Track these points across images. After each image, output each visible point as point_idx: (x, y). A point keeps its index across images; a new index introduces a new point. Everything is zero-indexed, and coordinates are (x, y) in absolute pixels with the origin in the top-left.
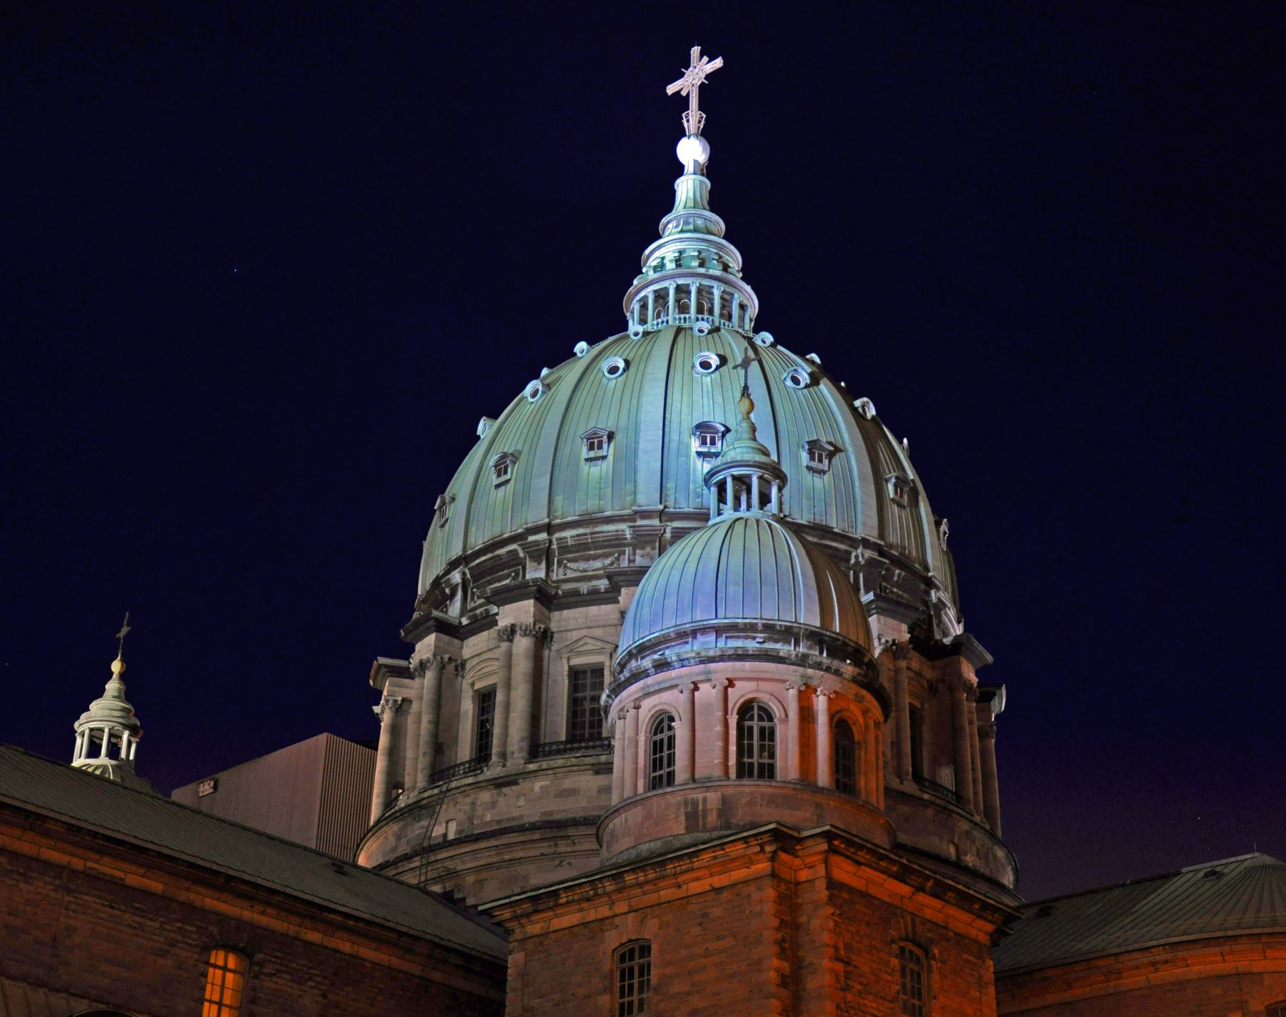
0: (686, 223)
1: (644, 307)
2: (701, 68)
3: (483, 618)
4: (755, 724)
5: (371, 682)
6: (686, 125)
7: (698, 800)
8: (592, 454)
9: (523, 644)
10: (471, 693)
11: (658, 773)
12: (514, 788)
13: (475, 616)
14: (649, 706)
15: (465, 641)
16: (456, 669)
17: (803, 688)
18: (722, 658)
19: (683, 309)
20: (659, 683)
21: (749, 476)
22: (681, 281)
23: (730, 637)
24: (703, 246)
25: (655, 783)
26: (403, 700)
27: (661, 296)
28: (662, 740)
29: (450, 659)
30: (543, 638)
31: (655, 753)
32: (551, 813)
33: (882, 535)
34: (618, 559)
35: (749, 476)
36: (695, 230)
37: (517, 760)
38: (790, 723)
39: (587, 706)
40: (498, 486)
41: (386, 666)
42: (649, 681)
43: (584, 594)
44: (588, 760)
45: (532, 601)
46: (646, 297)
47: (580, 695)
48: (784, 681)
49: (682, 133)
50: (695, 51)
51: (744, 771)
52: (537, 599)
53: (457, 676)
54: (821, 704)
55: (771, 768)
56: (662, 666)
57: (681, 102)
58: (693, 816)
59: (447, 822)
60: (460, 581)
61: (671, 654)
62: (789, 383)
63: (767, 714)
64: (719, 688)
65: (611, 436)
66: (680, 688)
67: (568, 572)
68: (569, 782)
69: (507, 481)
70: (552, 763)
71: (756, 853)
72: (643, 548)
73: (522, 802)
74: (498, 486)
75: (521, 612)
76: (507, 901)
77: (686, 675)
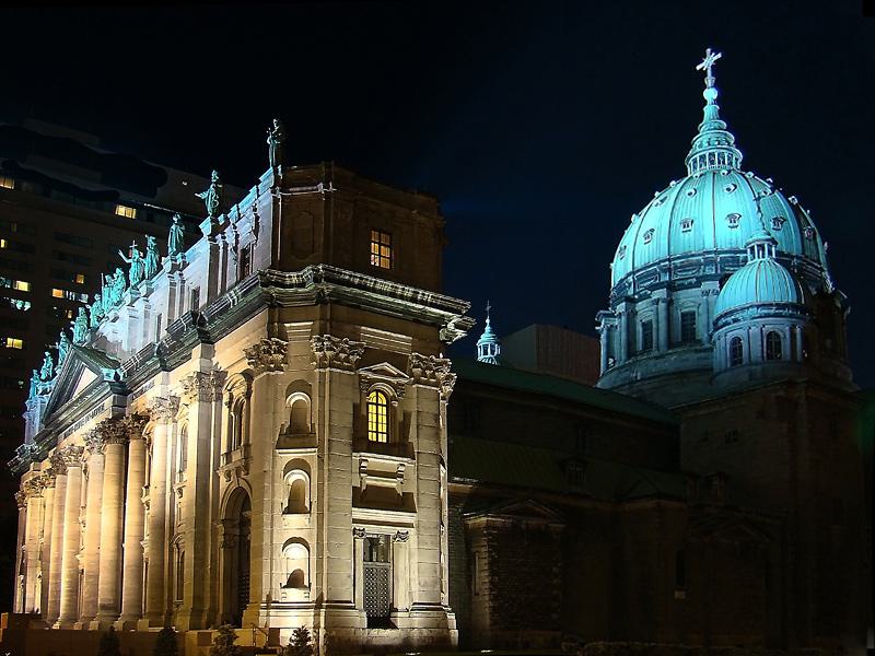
1: (695, 161)
2: (710, 60)
9: (662, 306)
14: (730, 336)
19: (712, 162)
27: (702, 157)
33: (803, 254)
37: (663, 349)
39: (689, 327)
49: (705, 87)
50: (709, 50)
54: (798, 330)
56: (735, 321)
57: (703, 73)
58: (752, 375)
63: (778, 336)
75: (661, 293)
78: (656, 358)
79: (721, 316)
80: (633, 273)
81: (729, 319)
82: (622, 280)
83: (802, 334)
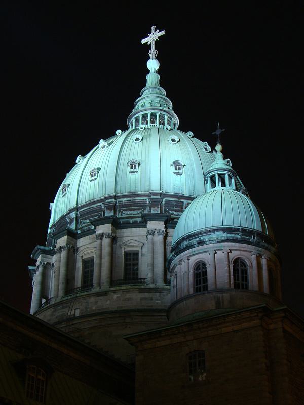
0: (153, 90)
1: (137, 120)
3: (87, 231)
4: (240, 268)
5: (32, 256)
6: (150, 55)
7: (220, 297)
8: (132, 170)
9: (106, 241)
10: (81, 260)
11: (199, 286)
12: (105, 297)
13: (84, 230)
14: (193, 260)
15: (78, 240)
16: (74, 251)
17: (258, 255)
18: (227, 241)
20: (197, 251)
21: (224, 174)
22: (153, 111)
23: (229, 233)
24: (160, 99)
25: (197, 290)
26: (47, 263)
27: (145, 117)
28: (200, 273)
29: (72, 246)
30: (114, 240)
31: (196, 278)
32: (122, 307)
34: (143, 211)
35: (224, 174)
36: (156, 93)
37: (105, 286)
38: (254, 268)
40: (91, 181)
41: (41, 249)
42: (195, 249)
43: (131, 223)
44: (136, 287)
45: (111, 225)
46: (139, 117)
47: (128, 262)
48: (251, 252)
49: (149, 58)
51: (236, 286)
52: (112, 224)
53: (75, 253)
54: (264, 261)
55: (247, 285)
56: (201, 243)
57: (148, 47)
58: (218, 303)
59: (75, 310)
60: (75, 216)
61: (205, 238)
62: (204, 150)
63: (243, 264)
64: (226, 253)
65: (139, 164)
66: (209, 252)
67: (123, 214)
68: (128, 296)
69: (95, 179)
70: (122, 288)
71: (255, 316)
72: (154, 207)
73: (108, 302)
74: (91, 181)
75: (105, 229)
76: (137, 334)
77: (213, 247)
78: (98, 294)
79: (183, 239)
80: (76, 209)
81: (195, 241)
82: (63, 217)
83: (268, 266)
